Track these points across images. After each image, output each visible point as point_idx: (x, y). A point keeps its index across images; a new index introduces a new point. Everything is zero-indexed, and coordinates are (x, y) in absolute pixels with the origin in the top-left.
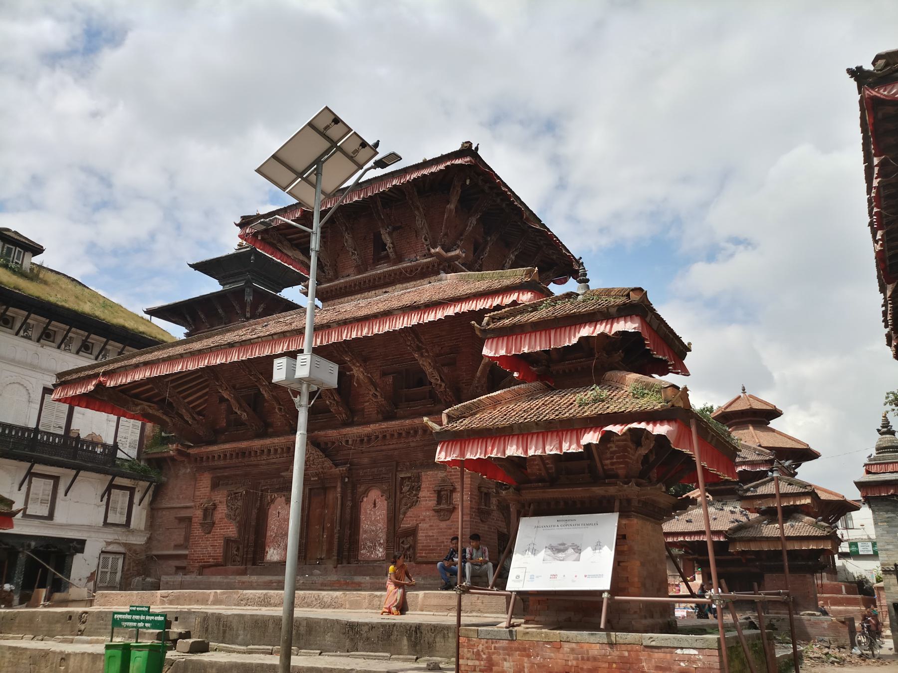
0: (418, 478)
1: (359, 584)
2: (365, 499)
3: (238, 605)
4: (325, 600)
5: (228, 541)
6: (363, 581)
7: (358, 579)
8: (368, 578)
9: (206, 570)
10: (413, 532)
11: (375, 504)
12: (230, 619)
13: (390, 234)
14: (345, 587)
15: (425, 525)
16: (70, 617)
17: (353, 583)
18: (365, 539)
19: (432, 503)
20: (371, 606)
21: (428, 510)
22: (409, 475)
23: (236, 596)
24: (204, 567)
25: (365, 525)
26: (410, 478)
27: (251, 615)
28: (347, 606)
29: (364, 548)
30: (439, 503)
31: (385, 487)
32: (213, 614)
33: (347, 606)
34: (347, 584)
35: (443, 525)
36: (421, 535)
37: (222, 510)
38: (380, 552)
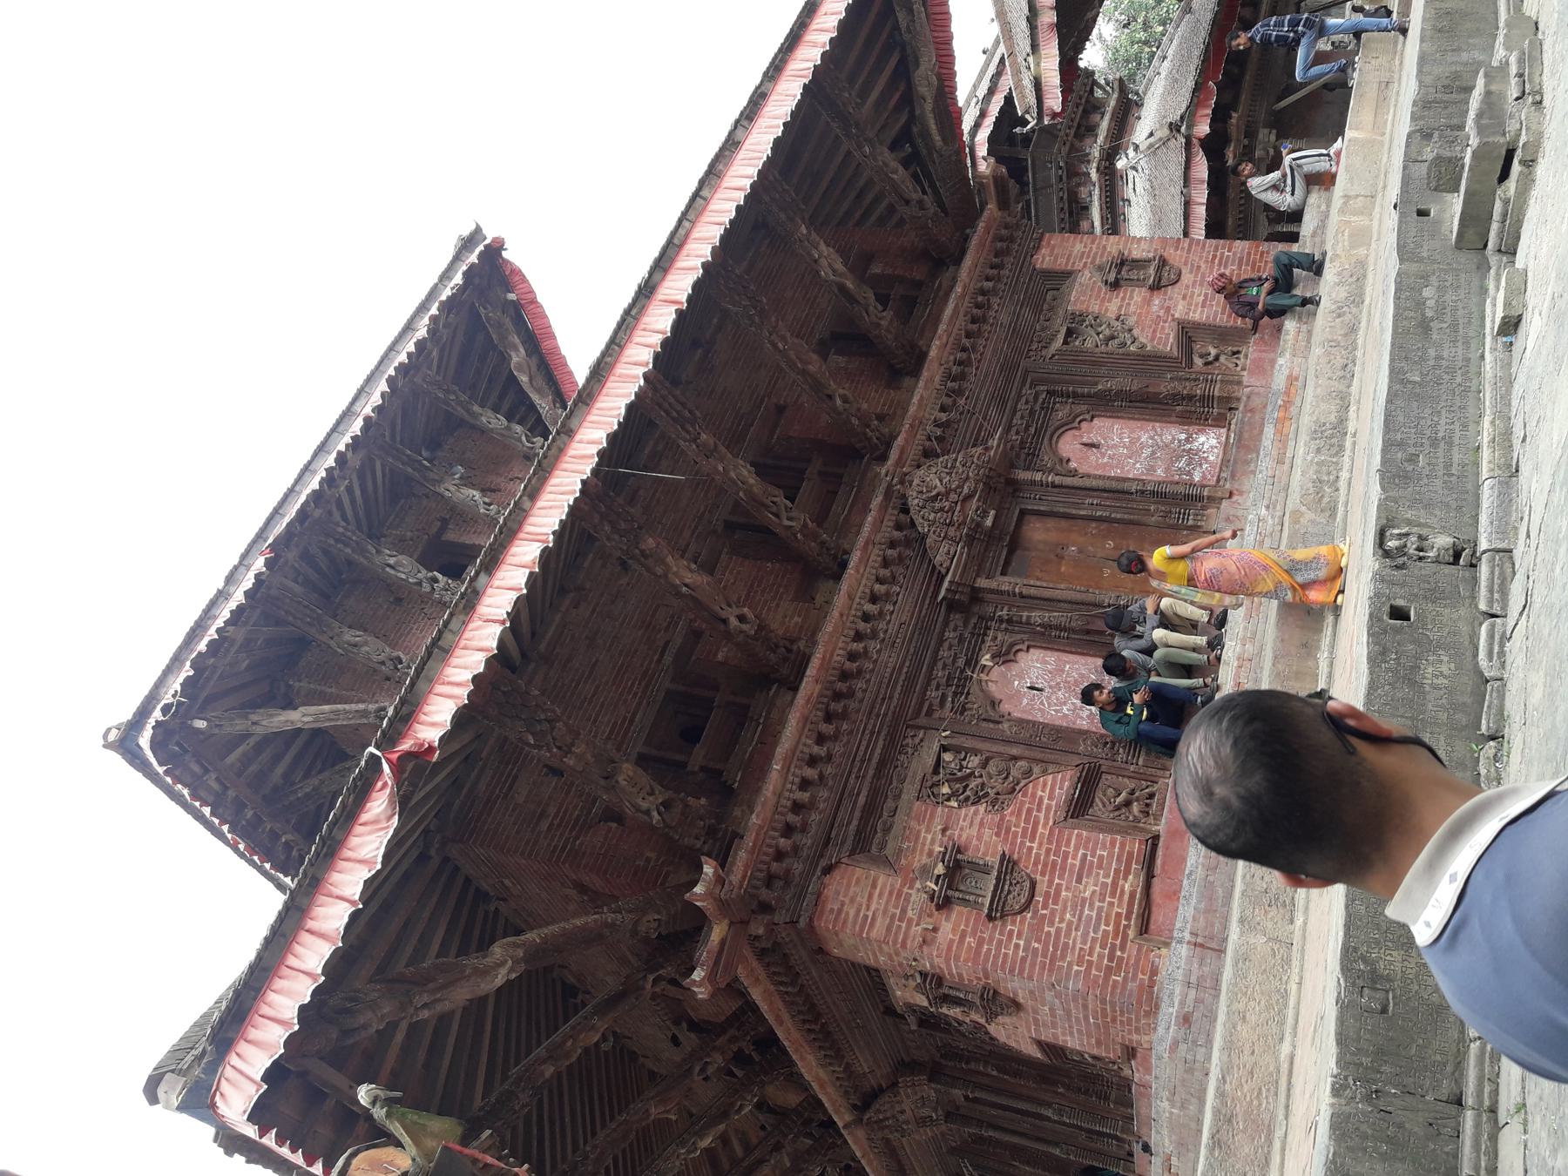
0: (1078, 318)
1: (1292, 379)
2: (1073, 465)
3: (1333, 515)
4: (1343, 295)
5: (1079, 807)
6: (1286, 372)
7: (1279, 381)
8: (1281, 361)
9: (1158, 917)
10: (1188, 333)
11: (1092, 445)
12: (1428, 80)
13: (467, 482)
14: (1293, 410)
15: (1180, 307)
16: (1399, 614)
17: (1287, 393)
18: (1167, 470)
19: (1138, 295)
20: (1367, 211)
21: (1148, 302)
22: (1063, 330)
23: (1309, 515)
24: (1144, 928)
25: (1135, 469)
26: (1069, 333)
27: (1422, 40)
28: (1362, 251)
29: (1189, 473)
30: (1139, 283)
31: (1062, 413)
32: (1414, 118)
33: (1362, 251)
34: (1287, 405)
35: (1187, 278)
36: (1197, 315)
37: (977, 830)
38: (1209, 442)
